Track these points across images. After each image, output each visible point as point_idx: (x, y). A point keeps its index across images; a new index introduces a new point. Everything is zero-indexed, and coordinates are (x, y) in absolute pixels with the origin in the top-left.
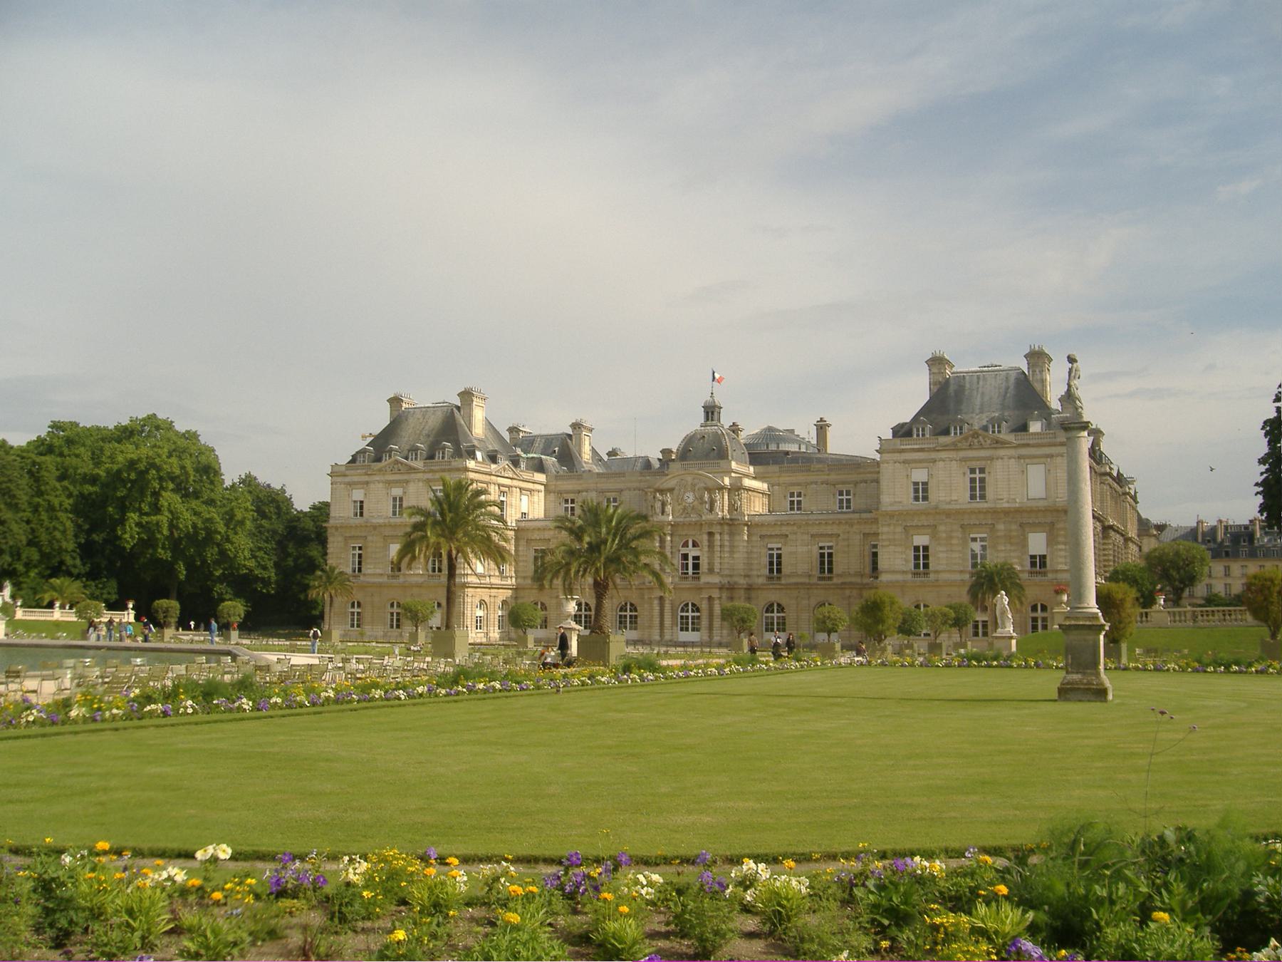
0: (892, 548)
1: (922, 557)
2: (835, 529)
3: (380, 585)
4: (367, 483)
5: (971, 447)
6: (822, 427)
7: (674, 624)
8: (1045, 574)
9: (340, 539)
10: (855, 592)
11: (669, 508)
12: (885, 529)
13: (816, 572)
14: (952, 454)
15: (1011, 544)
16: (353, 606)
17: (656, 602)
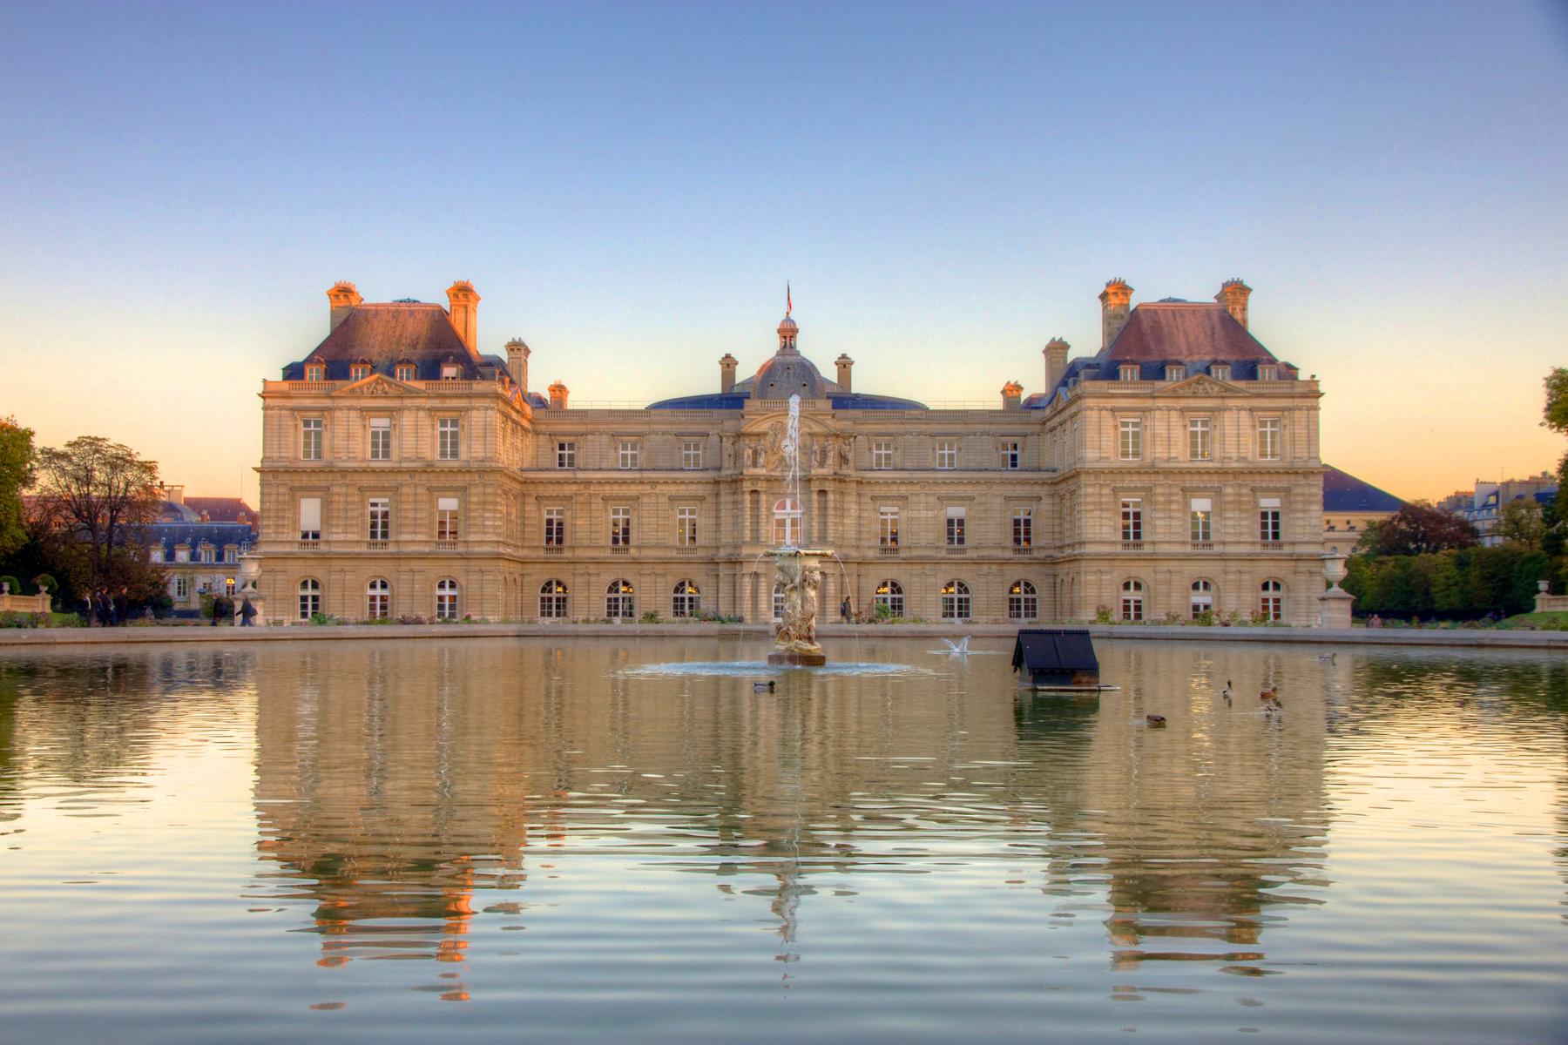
0: (1097, 513)
1: (1133, 528)
2: (968, 490)
3: (356, 557)
4: (329, 409)
5: (1195, 396)
6: (844, 364)
7: (769, 608)
8: (1280, 546)
9: (282, 490)
10: (994, 568)
11: (761, 460)
12: (1090, 490)
13: (944, 543)
14: (1172, 403)
15: (1241, 511)
16: (304, 585)
17: (747, 579)
